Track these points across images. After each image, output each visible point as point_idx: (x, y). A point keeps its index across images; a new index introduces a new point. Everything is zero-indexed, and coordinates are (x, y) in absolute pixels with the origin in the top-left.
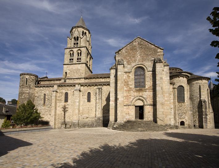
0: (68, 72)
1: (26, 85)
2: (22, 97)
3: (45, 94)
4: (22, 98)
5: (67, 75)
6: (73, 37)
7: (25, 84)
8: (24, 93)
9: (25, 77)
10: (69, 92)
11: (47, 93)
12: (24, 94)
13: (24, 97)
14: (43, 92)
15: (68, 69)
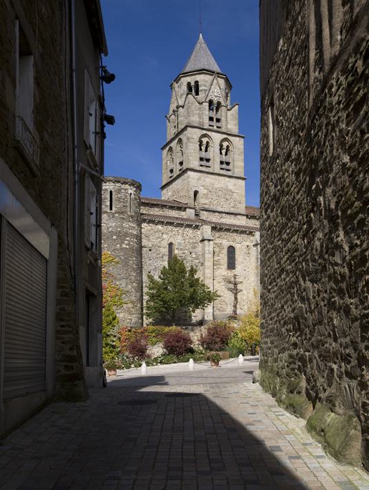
0: (202, 191)
1: (129, 213)
2: (124, 246)
3: (171, 245)
4: (122, 249)
5: (202, 201)
6: (207, 100)
7: (129, 209)
8: (126, 235)
9: (125, 190)
10: (237, 246)
11: (178, 241)
12: (128, 239)
13: (129, 244)
14: (165, 236)
15: (200, 182)
